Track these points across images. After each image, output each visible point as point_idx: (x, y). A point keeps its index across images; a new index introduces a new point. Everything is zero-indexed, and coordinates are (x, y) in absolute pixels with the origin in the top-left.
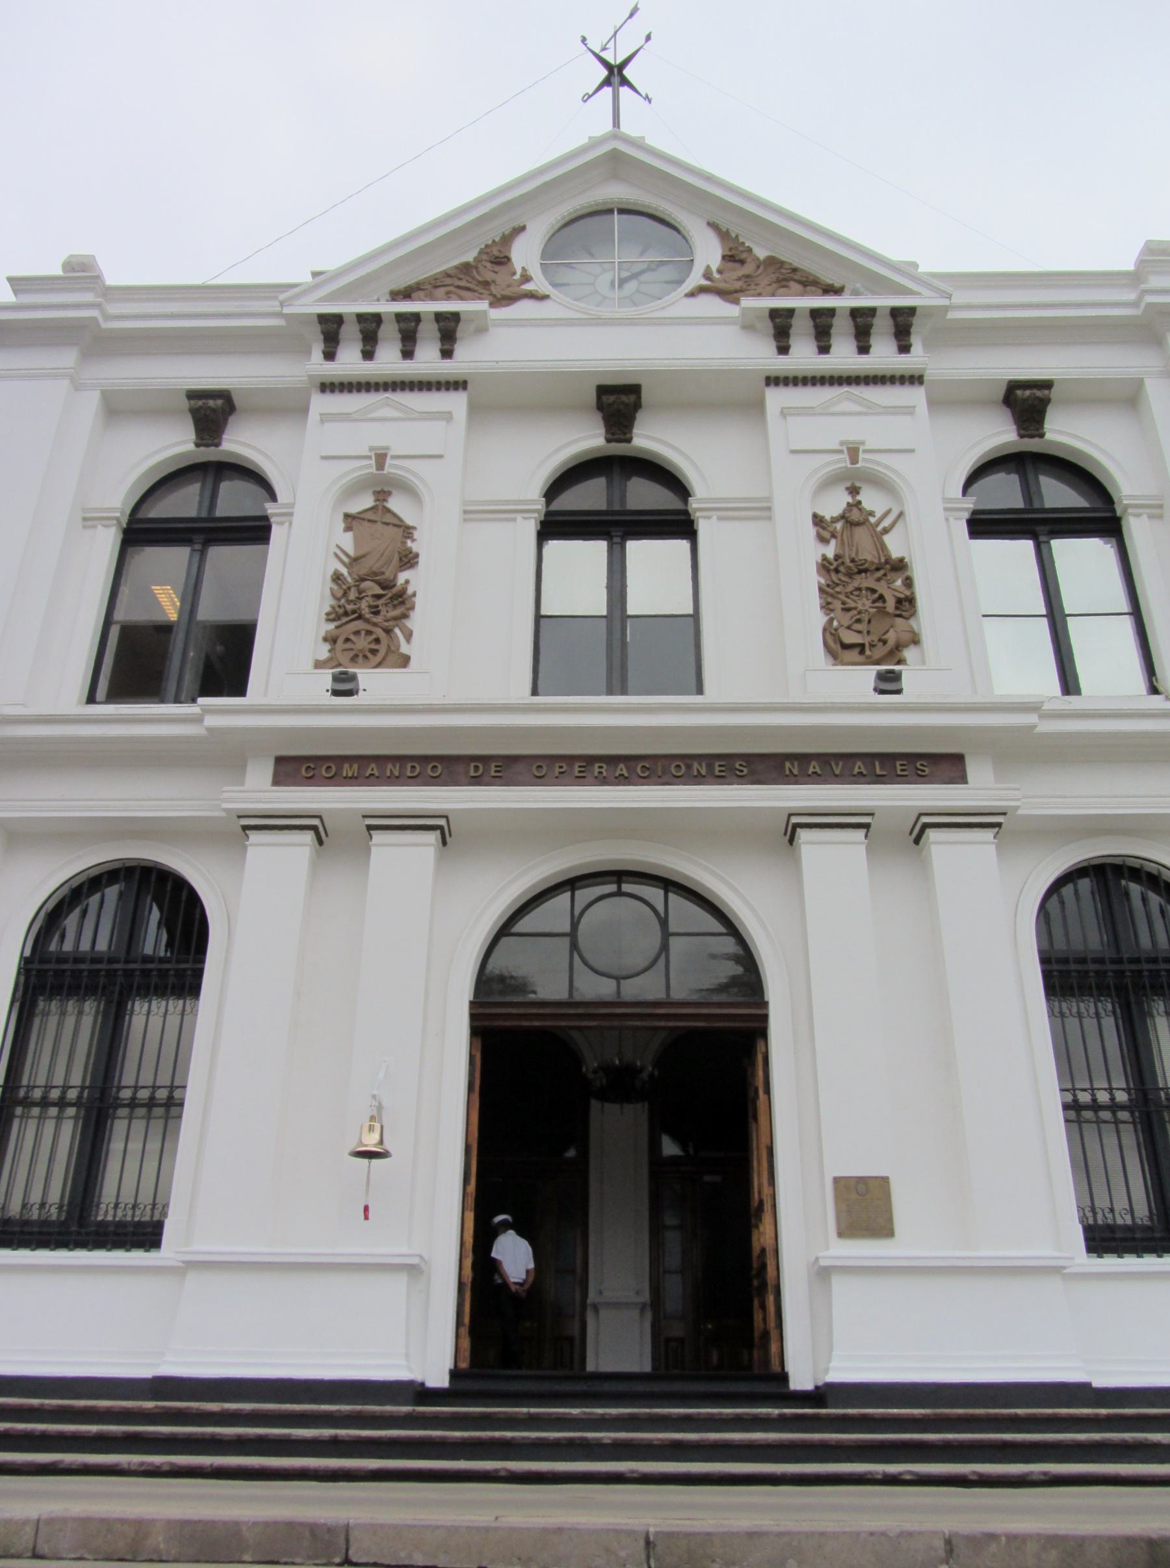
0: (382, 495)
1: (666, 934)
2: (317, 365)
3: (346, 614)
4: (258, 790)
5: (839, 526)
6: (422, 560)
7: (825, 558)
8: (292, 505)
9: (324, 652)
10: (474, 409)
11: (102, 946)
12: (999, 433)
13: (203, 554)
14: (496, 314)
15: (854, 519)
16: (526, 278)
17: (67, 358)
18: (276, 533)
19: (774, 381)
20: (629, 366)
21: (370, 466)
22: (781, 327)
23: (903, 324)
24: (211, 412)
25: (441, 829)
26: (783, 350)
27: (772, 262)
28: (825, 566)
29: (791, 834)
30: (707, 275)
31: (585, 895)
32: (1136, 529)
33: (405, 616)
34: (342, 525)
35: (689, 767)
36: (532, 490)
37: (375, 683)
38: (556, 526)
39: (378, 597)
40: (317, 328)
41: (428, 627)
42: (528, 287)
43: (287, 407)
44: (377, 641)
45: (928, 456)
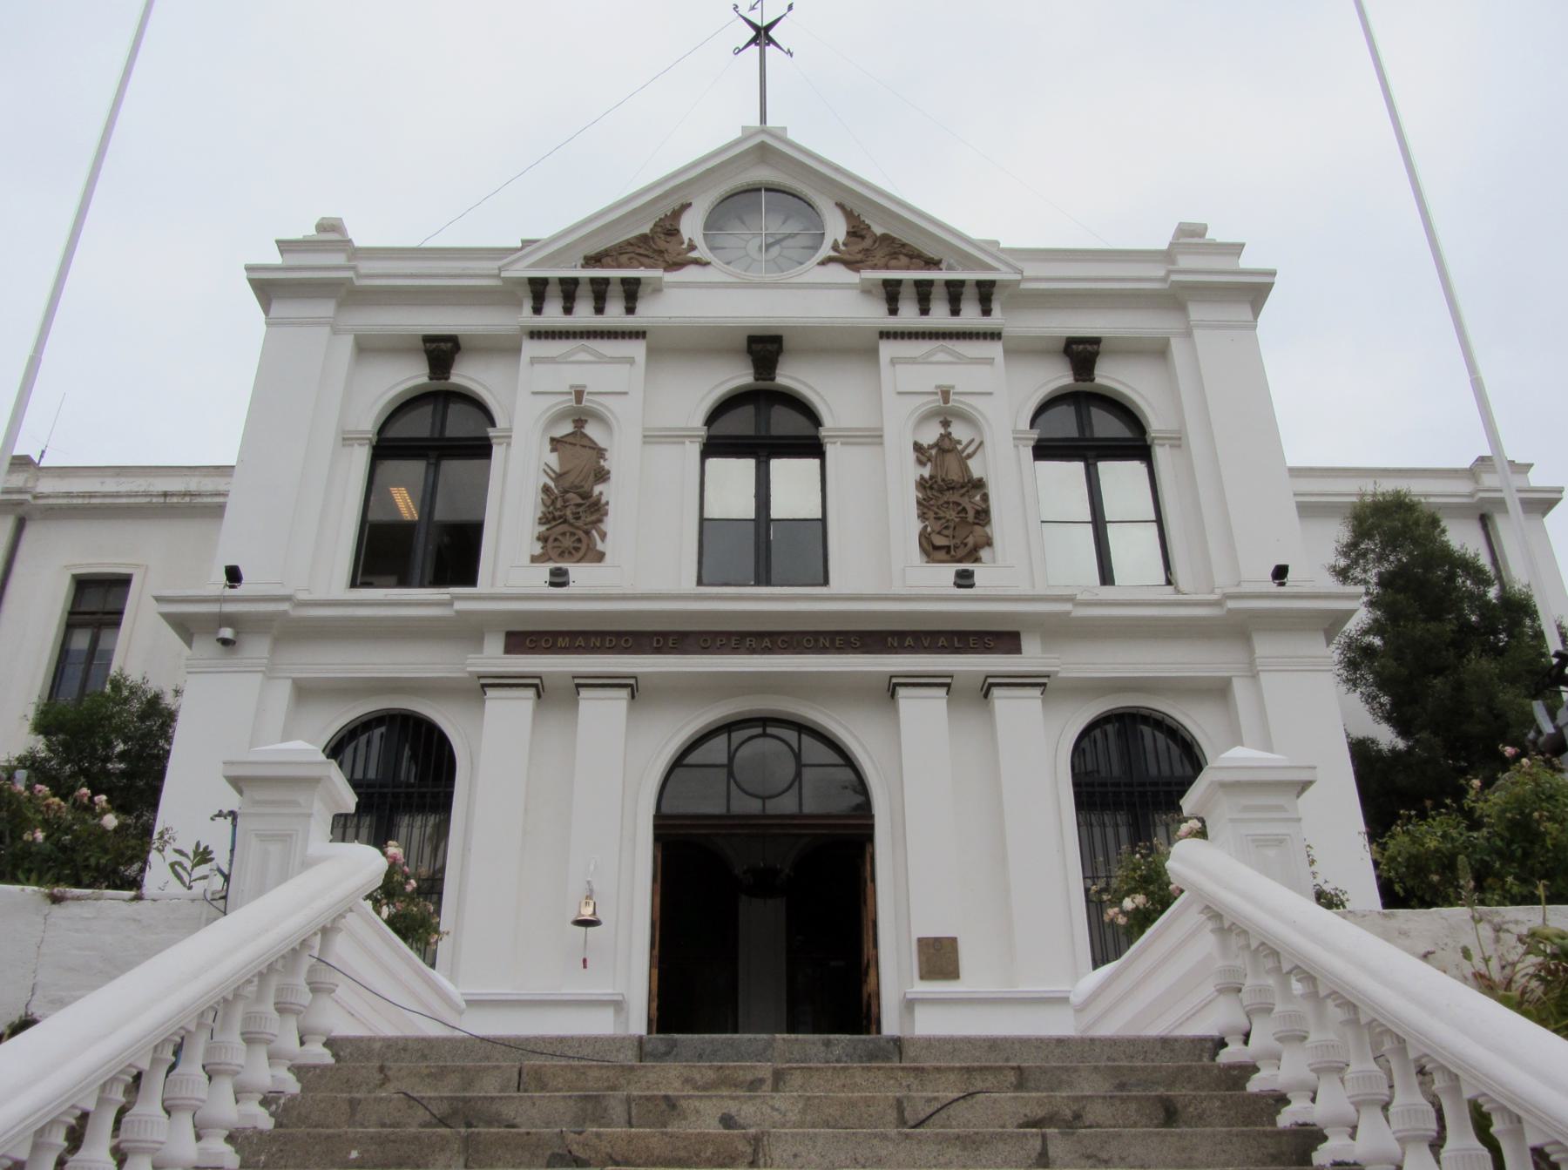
0: (580, 423)
1: (800, 765)
2: (526, 317)
3: (554, 519)
4: (494, 658)
5: (934, 452)
6: (613, 476)
7: (922, 478)
8: (510, 430)
9: (537, 549)
10: (652, 352)
11: (372, 775)
12: (1060, 377)
13: (437, 466)
14: (670, 277)
15: (946, 446)
16: (692, 247)
17: (326, 309)
18: (497, 452)
19: (886, 335)
20: (773, 322)
21: (570, 401)
22: (891, 294)
23: (986, 293)
24: (442, 352)
25: (632, 686)
26: (893, 311)
27: (886, 238)
28: (922, 484)
29: (892, 690)
30: (835, 247)
31: (738, 736)
32: (1161, 454)
33: (600, 521)
34: (548, 447)
35: (816, 641)
36: (697, 420)
37: (581, 575)
38: (715, 447)
39: (579, 505)
40: (528, 288)
41: (621, 527)
42: (693, 255)
43: (504, 348)
44: (579, 540)
45: (1002, 395)
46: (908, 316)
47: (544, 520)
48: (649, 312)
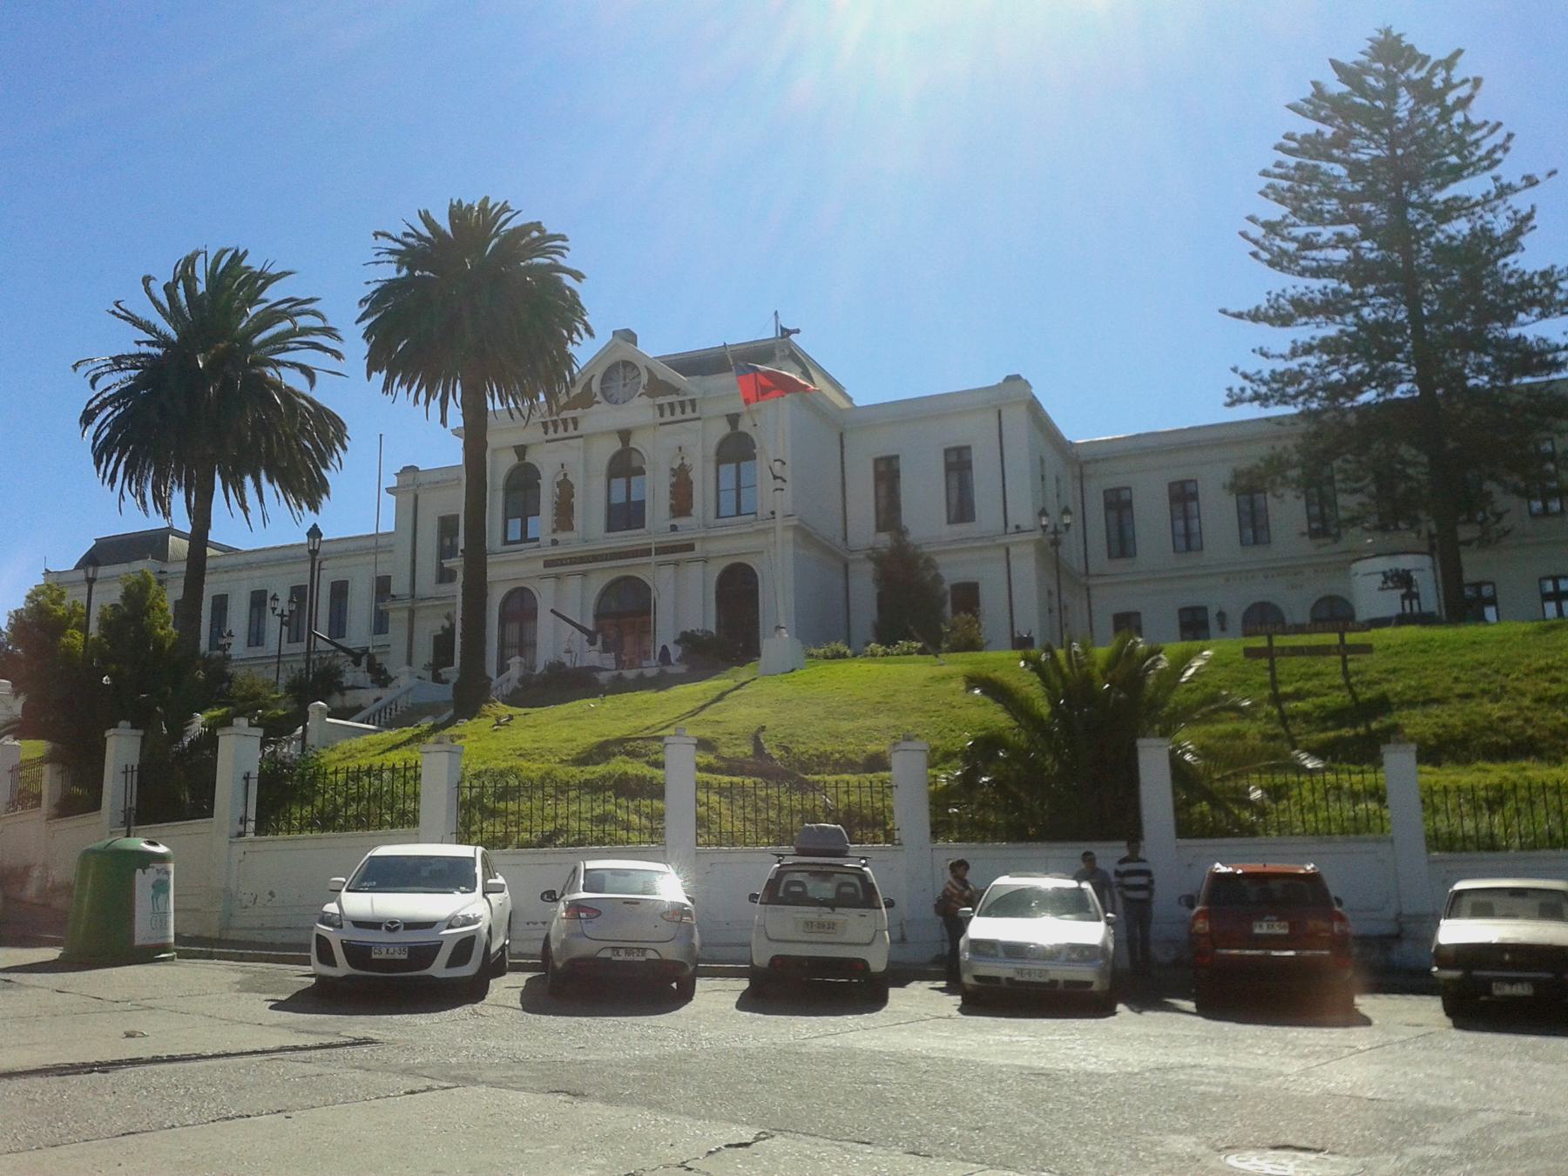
22: (661, 407)
23: (693, 402)
46: (668, 417)
48: (584, 427)
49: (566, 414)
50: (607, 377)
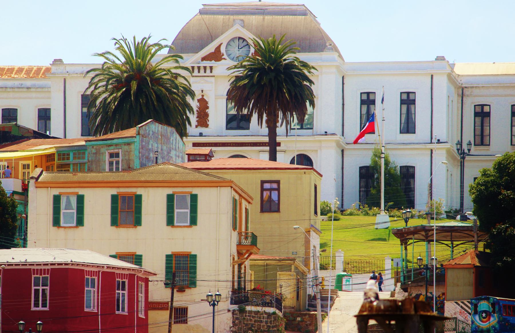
9: (196, 124)
42: (223, 57)
47: (197, 118)
49: (208, 64)
50: (228, 44)
